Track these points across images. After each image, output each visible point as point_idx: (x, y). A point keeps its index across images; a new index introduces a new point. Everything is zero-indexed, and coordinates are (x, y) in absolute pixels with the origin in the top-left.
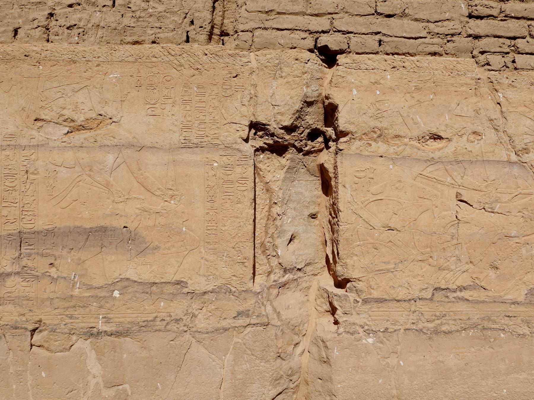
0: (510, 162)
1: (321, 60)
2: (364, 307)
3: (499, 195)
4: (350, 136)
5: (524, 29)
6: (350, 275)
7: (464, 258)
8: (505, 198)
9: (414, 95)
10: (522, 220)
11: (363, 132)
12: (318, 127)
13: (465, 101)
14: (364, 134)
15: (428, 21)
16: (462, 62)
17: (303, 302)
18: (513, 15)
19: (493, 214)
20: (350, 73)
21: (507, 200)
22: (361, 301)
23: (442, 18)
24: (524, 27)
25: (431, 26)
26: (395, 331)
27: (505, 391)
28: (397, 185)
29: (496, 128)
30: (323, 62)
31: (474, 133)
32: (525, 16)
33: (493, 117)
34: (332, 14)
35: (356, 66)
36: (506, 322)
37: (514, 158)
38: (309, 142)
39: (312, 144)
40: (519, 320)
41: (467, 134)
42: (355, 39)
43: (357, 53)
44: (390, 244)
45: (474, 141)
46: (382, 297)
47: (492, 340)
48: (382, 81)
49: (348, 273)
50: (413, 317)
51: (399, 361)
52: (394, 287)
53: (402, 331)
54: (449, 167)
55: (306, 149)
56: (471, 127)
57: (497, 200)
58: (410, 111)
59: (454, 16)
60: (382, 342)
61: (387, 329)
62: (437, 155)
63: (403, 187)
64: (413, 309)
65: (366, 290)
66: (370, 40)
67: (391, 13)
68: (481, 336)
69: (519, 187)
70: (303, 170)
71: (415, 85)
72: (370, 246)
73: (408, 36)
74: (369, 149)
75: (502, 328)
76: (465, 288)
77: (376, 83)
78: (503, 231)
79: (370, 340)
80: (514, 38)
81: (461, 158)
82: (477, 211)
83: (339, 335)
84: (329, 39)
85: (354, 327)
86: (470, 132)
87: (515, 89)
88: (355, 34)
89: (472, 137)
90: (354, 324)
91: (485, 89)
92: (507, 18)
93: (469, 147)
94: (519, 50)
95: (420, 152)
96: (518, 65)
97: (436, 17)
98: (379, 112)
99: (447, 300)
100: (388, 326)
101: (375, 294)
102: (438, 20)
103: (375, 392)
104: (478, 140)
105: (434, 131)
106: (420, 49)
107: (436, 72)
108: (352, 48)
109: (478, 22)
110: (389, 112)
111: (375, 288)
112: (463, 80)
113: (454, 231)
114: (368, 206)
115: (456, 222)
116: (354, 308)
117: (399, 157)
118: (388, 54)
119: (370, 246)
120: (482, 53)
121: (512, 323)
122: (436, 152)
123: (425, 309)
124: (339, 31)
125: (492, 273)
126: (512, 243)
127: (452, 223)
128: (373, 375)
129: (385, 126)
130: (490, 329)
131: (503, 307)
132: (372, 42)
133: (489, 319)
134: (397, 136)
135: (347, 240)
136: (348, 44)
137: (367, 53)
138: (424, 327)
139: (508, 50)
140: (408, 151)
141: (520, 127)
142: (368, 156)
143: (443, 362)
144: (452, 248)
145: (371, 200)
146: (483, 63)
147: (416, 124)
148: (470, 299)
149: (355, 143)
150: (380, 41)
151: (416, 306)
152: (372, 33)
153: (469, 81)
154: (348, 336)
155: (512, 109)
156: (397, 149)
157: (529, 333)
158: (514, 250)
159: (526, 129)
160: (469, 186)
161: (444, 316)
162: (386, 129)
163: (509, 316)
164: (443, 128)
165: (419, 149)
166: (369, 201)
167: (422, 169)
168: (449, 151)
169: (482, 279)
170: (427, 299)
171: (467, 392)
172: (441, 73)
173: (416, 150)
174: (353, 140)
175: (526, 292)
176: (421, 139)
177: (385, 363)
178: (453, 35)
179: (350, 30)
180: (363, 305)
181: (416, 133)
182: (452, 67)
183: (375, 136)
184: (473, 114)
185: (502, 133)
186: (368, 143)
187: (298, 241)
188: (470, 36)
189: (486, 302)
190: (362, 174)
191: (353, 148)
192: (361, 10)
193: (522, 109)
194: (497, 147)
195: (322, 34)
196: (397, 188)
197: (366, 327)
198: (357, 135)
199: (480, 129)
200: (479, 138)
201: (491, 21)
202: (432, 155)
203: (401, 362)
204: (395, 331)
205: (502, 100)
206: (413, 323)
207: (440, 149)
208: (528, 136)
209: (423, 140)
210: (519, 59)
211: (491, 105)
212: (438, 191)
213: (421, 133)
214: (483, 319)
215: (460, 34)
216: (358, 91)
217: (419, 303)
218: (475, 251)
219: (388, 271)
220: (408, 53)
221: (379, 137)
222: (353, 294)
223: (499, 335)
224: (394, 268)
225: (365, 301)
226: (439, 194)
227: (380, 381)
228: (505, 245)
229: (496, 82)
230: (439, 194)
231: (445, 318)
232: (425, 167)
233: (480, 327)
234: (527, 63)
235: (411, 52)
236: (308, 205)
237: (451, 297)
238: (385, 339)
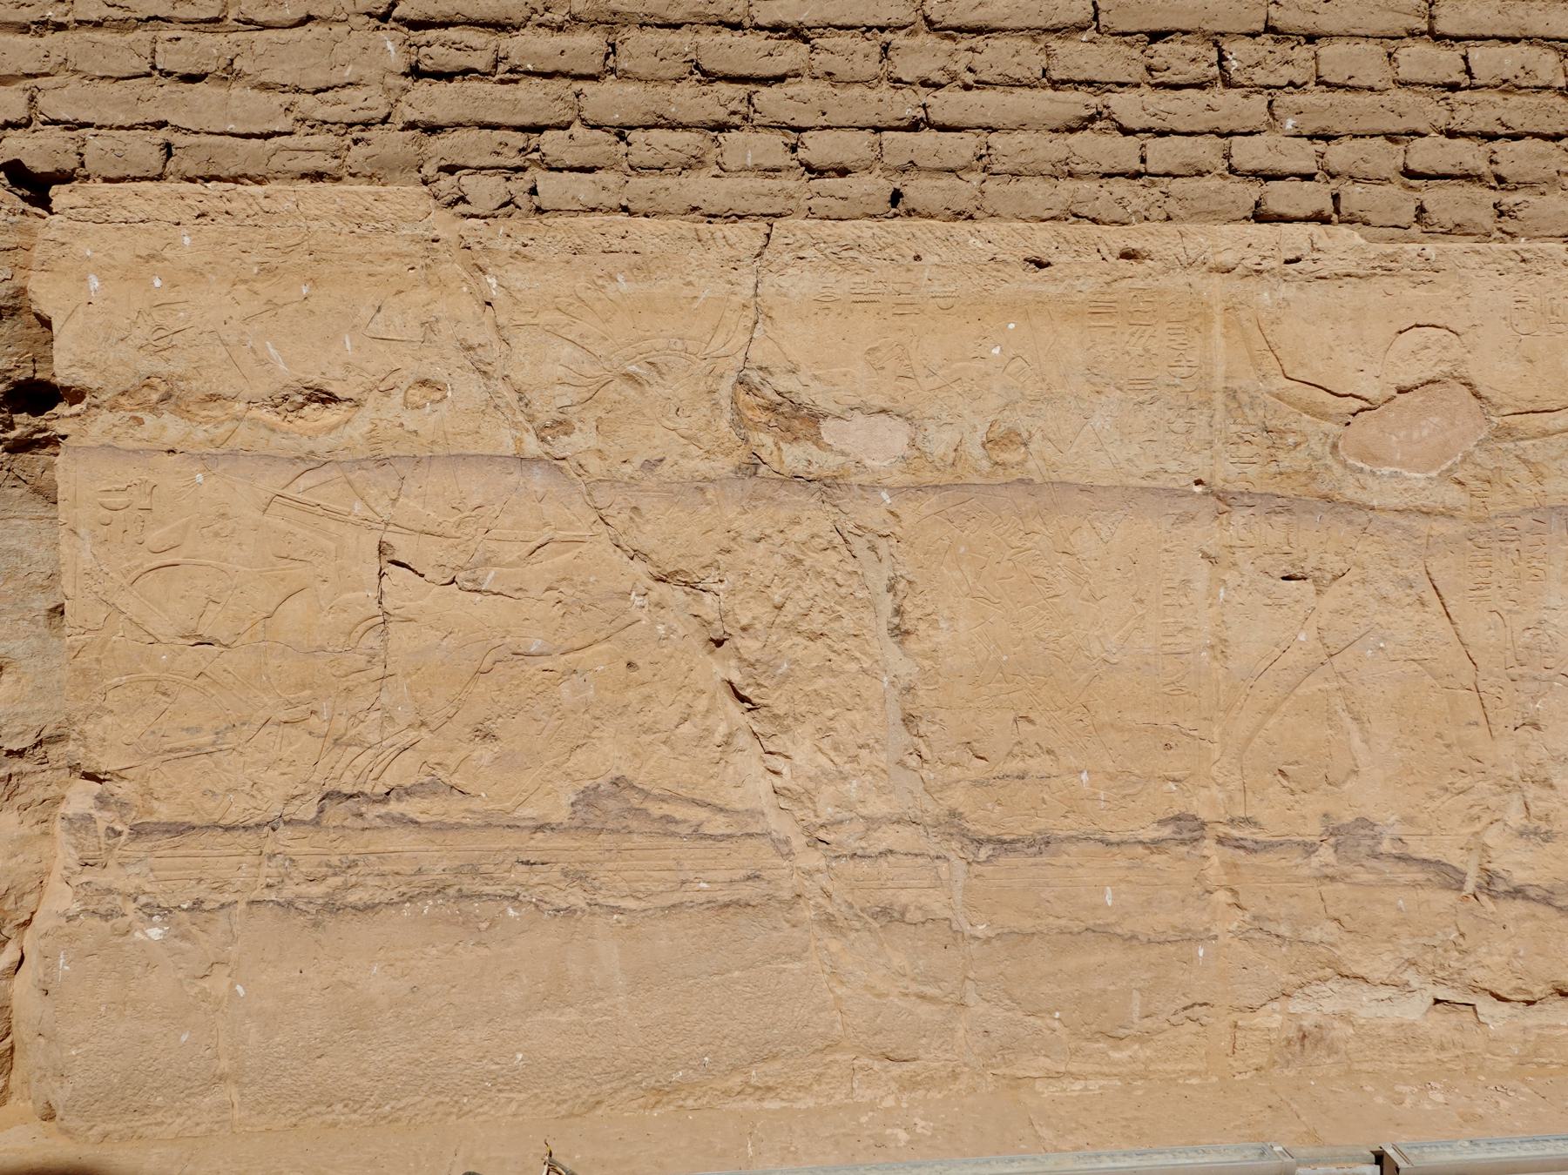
0: (522, 460)
1: (23, 198)
2: (134, 846)
3: (493, 545)
4: (88, 399)
5: (560, 105)
6: (93, 764)
7: (404, 715)
8: (513, 552)
9: (258, 286)
10: (558, 610)
11: (121, 389)
12: (38, 376)
13: (396, 299)
14: (123, 394)
15: (298, 90)
16: (389, 197)
17: (25, 841)
18: (529, 66)
19: (478, 597)
20: (81, 234)
21: (514, 557)
22: (126, 831)
23: (335, 81)
24: (560, 98)
25: (306, 102)
26: (223, 906)
27: (520, 1056)
28: (217, 526)
29: (484, 368)
30: (33, 205)
31: (424, 383)
32: (564, 68)
33: (474, 341)
34: (35, 76)
35: (96, 216)
36: (522, 879)
37: (532, 446)
38: (21, 418)
39: (36, 421)
40: (555, 873)
41: (404, 387)
42: (97, 142)
43: (106, 180)
44: (201, 681)
45: (424, 406)
46: (180, 819)
47: (484, 926)
48: (168, 253)
49: (90, 759)
50: (270, 870)
51: (232, 985)
52: (214, 794)
53: (242, 906)
54: (355, 476)
55: (12, 435)
56: (413, 369)
57: (488, 560)
58: (247, 329)
59: (369, 73)
60: (184, 937)
61: (197, 904)
62: (323, 444)
63: (234, 531)
64: (267, 850)
65: (139, 803)
66: (138, 144)
67: (194, 71)
68: (453, 914)
69: (547, 524)
70: (17, 492)
71: (259, 259)
72: (148, 687)
73: (242, 131)
74: (139, 433)
75: (509, 893)
76: (409, 792)
77: (153, 257)
78: (508, 639)
79: (155, 933)
80: (538, 129)
81: (388, 451)
82: (437, 589)
83: (69, 919)
84: (24, 142)
85: (109, 898)
86: (411, 381)
87: (531, 264)
88: (100, 128)
89: (417, 395)
90: (110, 891)
91: (452, 268)
92: (516, 76)
93: (411, 420)
94: (548, 159)
95: (276, 439)
96: (543, 199)
97: (318, 78)
98: (162, 333)
99: (359, 823)
100: (202, 895)
101: (164, 812)
102: (322, 85)
103: (170, 1067)
104: (432, 402)
105: (316, 379)
106: (276, 163)
107: (315, 225)
108: (91, 167)
109: (440, 87)
110: (190, 333)
111: (162, 796)
112: (390, 243)
113: (376, 644)
114: (140, 582)
115: (380, 619)
116: (110, 849)
117: (220, 451)
118: (191, 180)
119: (148, 687)
120: (451, 170)
121: (536, 880)
122: (321, 438)
123: (299, 848)
124: (55, 122)
125: (484, 753)
126: (532, 670)
127: (370, 623)
128: (165, 1022)
129: (179, 371)
130: (480, 896)
131: (512, 839)
132: (143, 150)
133: (475, 871)
134: (213, 398)
135: (84, 672)
136: (81, 155)
137: (134, 179)
138: (298, 897)
139: (518, 161)
140: (244, 435)
141: (548, 365)
142: (135, 452)
143: (350, 985)
144: (373, 687)
145: (147, 566)
146: (449, 198)
147: (262, 362)
148: (422, 818)
149: (100, 418)
150: (168, 148)
151: (276, 841)
152: (145, 126)
153: (405, 247)
154: (96, 922)
155: (522, 319)
156: (212, 430)
157: (583, 905)
158: (539, 689)
159: (560, 371)
160: (411, 525)
161: (354, 864)
162: (181, 378)
163: (527, 863)
164: (338, 372)
165: (273, 430)
166: (141, 570)
167: (285, 482)
168: (356, 435)
169: (452, 768)
170: (303, 823)
171: (417, 1062)
172: (328, 226)
173: (264, 433)
174: (94, 410)
175: (574, 798)
176: (279, 402)
177: (196, 990)
178: (367, 125)
179: (83, 119)
180: (133, 840)
181: (263, 388)
182: (359, 209)
183: (155, 397)
184: (418, 333)
185: (500, 383)
186: (135, 418)
187: (14, 678)
188: (411, 126)
189: (465, 826)
190: (121, 499)
191: (94, 430)
192: (114, 66)
193: (545, 317)
194: (487, 418)
195: (9, 131)
196: (217, 535)
197: (143, 900)
198: (104, 397)
199: (438, 373)
200: (438, 395)
201: (473, 86)
202: (309, 445)
203: (239, 988)
204: (223, 906)
205: (495, 294)
206: (269, 886)
207: (332, 428)
208: (566, 388)
209: (286, 405)
210: (552, 187)
211: (468, 308)
212: (330, 539)
213: (278, 386)
214: (458, 872)
215: (384, 121)
216: (102, 280)
217: (284, 833)
218: (431, 694)
219: (198, 751)
220: (245, 176)
221: (164, 399)
222: (107, 814)
223: (504, 911)
224: (214, 743)
225: (138, 832)
226: (332, 546)
227: (184, 1038)
228: (513, 677)
229: (478, 247)
230: (332, 546)
231: (356, 870)
232: (290, 478)
233: (452, 892)
234: (569, 195)
235: (251, 173)
236: (46, 583)
237: (369, 816)
238: (194, 930)
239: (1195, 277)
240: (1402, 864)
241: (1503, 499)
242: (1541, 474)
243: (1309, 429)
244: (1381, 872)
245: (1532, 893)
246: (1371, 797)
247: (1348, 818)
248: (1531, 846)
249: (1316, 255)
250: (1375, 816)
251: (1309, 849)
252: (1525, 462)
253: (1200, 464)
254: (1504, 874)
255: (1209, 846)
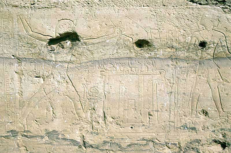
239: (10, 8)
240: (64, 140)
241: (84, 59)
242: (93, 53)
243: (38, 43)
244: (59, 142)
245: (94, 146)
246: (56, 125)
247: (51, 130)
248: (93, 136)
249: (39, 3)
250: (57, 129)
251: (42, 137)
252: (89, 50)
253: (13, 52)
254: (87, 142)
255: (19, 137)
